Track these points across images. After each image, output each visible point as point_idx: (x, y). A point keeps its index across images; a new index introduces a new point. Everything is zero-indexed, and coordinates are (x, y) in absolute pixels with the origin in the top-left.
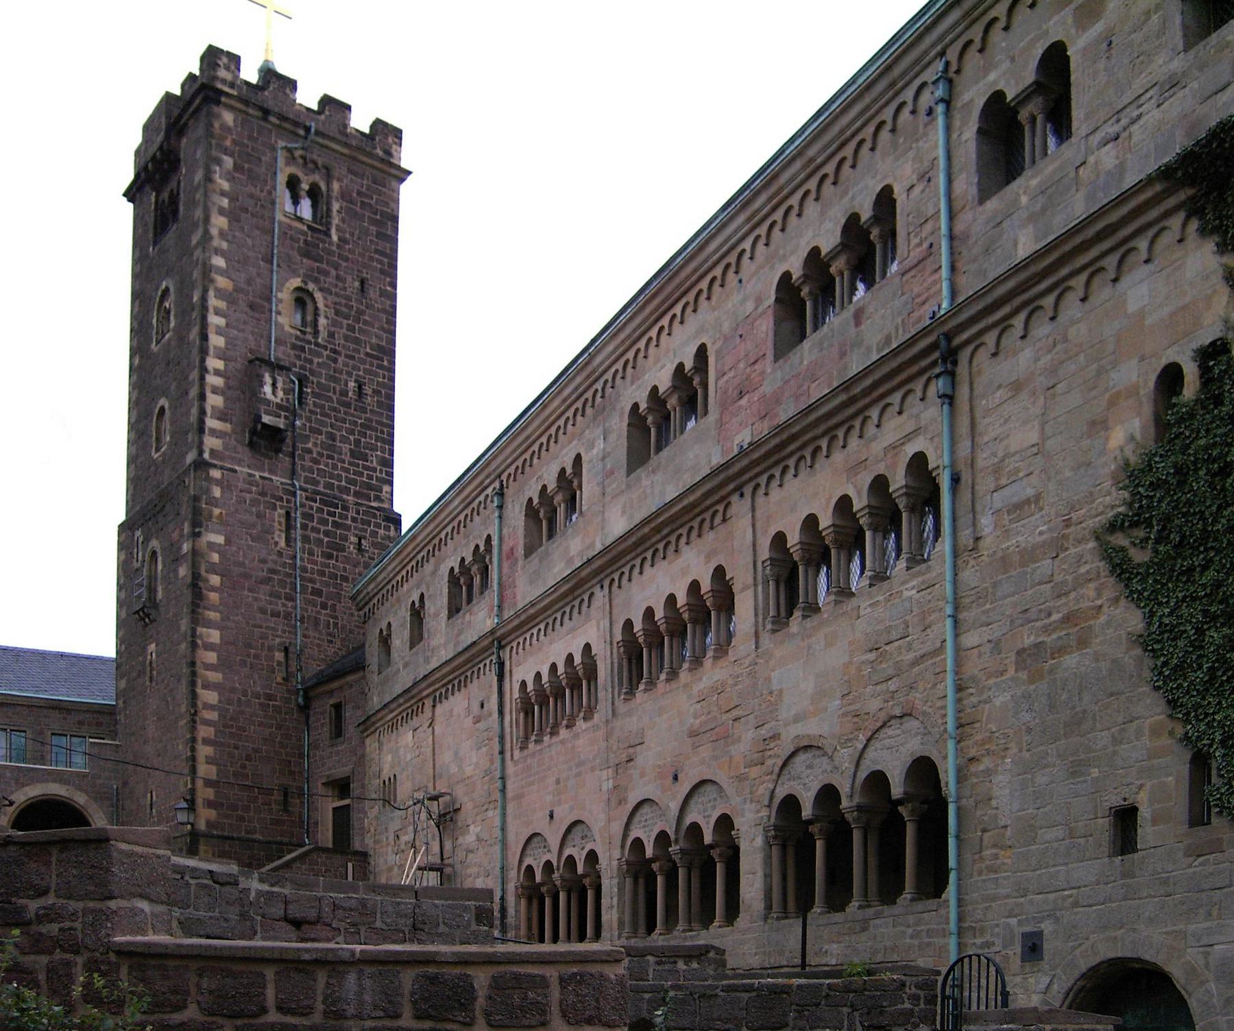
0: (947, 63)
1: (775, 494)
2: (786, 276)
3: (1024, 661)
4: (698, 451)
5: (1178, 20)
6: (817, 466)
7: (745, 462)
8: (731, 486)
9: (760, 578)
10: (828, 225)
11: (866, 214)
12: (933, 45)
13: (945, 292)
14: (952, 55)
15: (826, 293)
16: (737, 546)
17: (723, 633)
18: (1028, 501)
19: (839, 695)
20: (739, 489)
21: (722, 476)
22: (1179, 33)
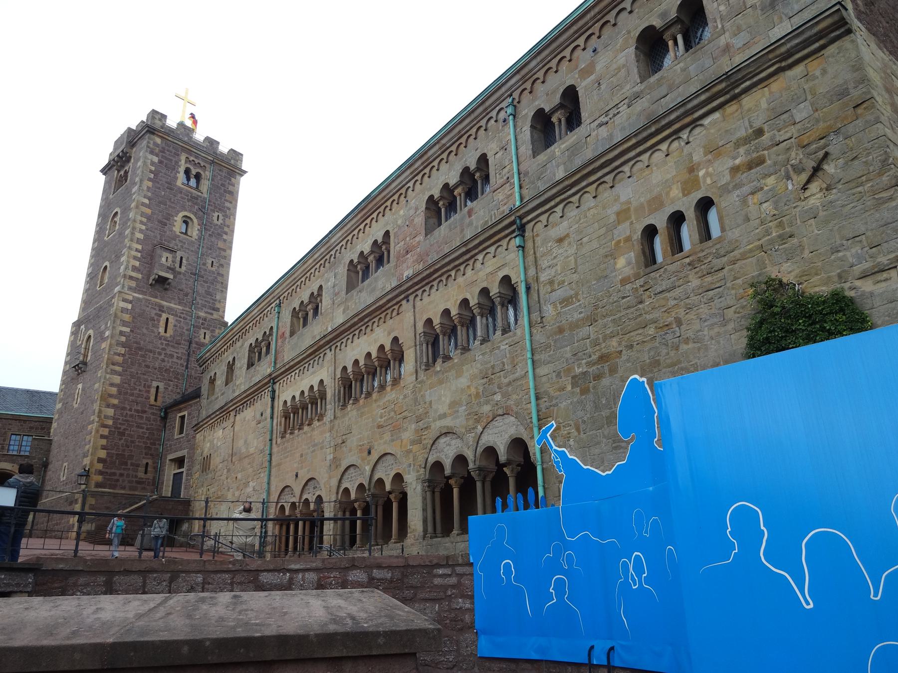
0: (514, 99)
1: (426, 299)
2: (431, 197)
3: (577, 382)
4: (383, 281)
5: (636, 71)
6: (449, 284)
7: (410, 284)
8: (403, 296)
9: (418, 343)
10: (453, 173)
11: (473, 167)
12: (506, 92)
13: (517, 197)
14: (516, 95)
15: (452, 207)
16: (405, 326)
17: (396, 372)
18: (571, 297)
19: (465, 403)
20: (407, 298)
21: (397, 291)
22: (637, 76)
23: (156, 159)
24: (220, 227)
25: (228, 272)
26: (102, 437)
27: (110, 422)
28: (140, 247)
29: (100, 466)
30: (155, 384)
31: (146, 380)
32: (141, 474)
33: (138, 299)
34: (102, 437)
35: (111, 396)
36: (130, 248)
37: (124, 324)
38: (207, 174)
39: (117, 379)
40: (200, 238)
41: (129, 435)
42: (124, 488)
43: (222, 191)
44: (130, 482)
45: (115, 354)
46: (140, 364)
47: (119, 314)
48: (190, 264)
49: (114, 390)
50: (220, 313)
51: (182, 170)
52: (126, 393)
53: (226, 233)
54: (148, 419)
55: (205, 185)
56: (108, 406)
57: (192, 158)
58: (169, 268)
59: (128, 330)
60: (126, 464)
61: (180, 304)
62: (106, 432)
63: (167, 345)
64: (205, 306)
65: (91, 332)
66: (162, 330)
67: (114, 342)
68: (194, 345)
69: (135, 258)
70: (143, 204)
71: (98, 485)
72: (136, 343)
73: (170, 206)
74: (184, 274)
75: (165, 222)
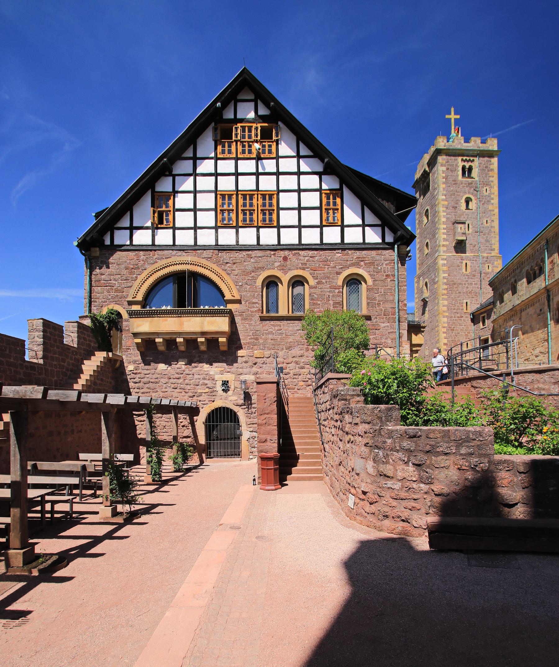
24: (489, 196)
37: (444, 272)
40: (477, 208)
45: (443, 289)
47: (441, 267)
55: (475, 173)
58: (463, 234)
72: (452, 281)
74: (471, 234)
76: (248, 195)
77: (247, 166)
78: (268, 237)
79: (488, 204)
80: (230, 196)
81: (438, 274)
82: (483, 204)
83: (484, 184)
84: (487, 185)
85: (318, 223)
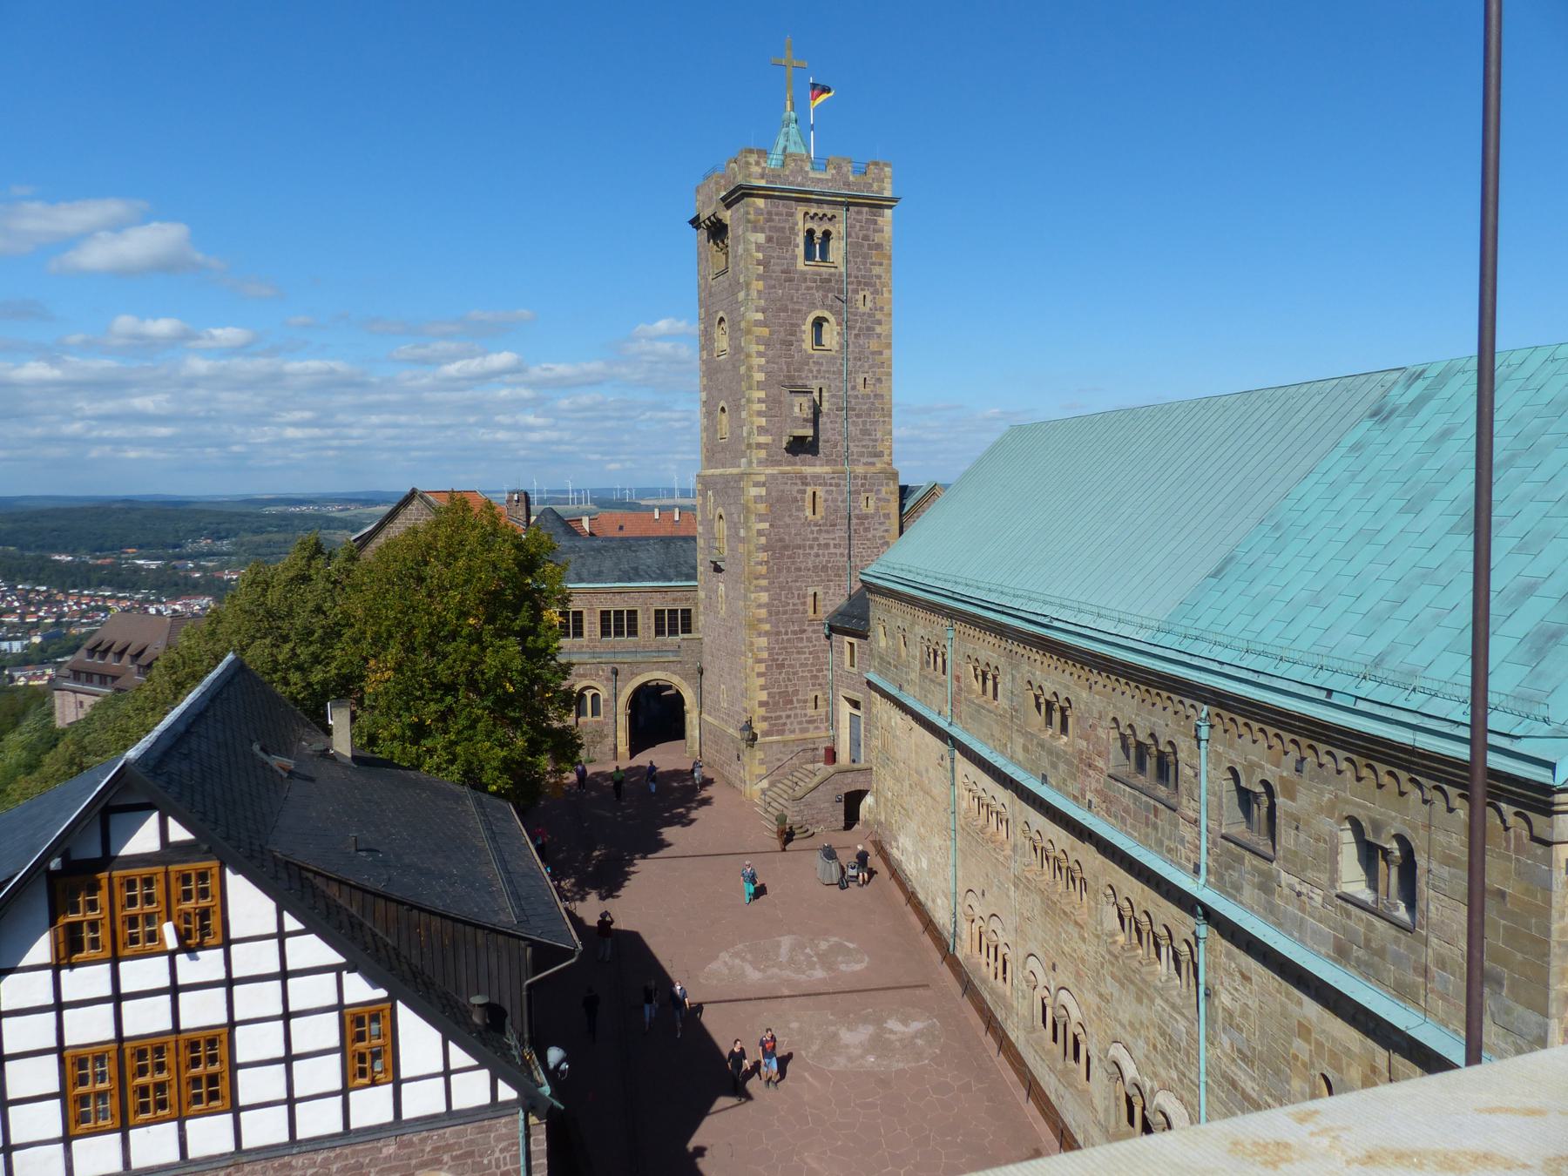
23: (761, 238)
24: (870, 315)
25: (890, 389)
26: (759, 675)
27: (765, 655)
28: (762, 394)
29: (762, 711)
30: (811, 591)
31: (800, 589)
32: (811, 712)
33: (773, 475)
34: (759, 675)
35: (760, 621)
36: (749, 401)
37: (761, 518)
38: (838, 229)
39: (764, 597)
40: (842, 347)
41: (791, 666)
42: (793, 731)
43: (865, 250)
44: (800, 723)
46: (788, 570)
47: (752, 505)
48: (833, 396)
49: (763, 612)
50: (886, 458)
51: (800, 240)
52: (778, 613)
53: (879, 323)
54: (809, 640)
55: (837, 250)
56: (759, 635)
57: (812, 211)
58: (805, 420)
59: (765, 526)
60: (791, 702)
61: (828, 463)
62: (762, 668)
63: (820, 531)
64: (862, 454)
65: (720, 510)
66: (809, 512)
67: (752, 548)
68: (854, 521)
69: (759, 414)
70: (758, 323)
71: (766, 734)
73: (793, 311)
75: (789, 342)
76: (150, 1050)
77: (142, 973)
78: (210, 1135)
79: (868, 337)
80: (99, 1059)
81: (747, 518)
82: (857, 336)
83: (859, 283)
84: (866, 284)
85: (338, 1086)
